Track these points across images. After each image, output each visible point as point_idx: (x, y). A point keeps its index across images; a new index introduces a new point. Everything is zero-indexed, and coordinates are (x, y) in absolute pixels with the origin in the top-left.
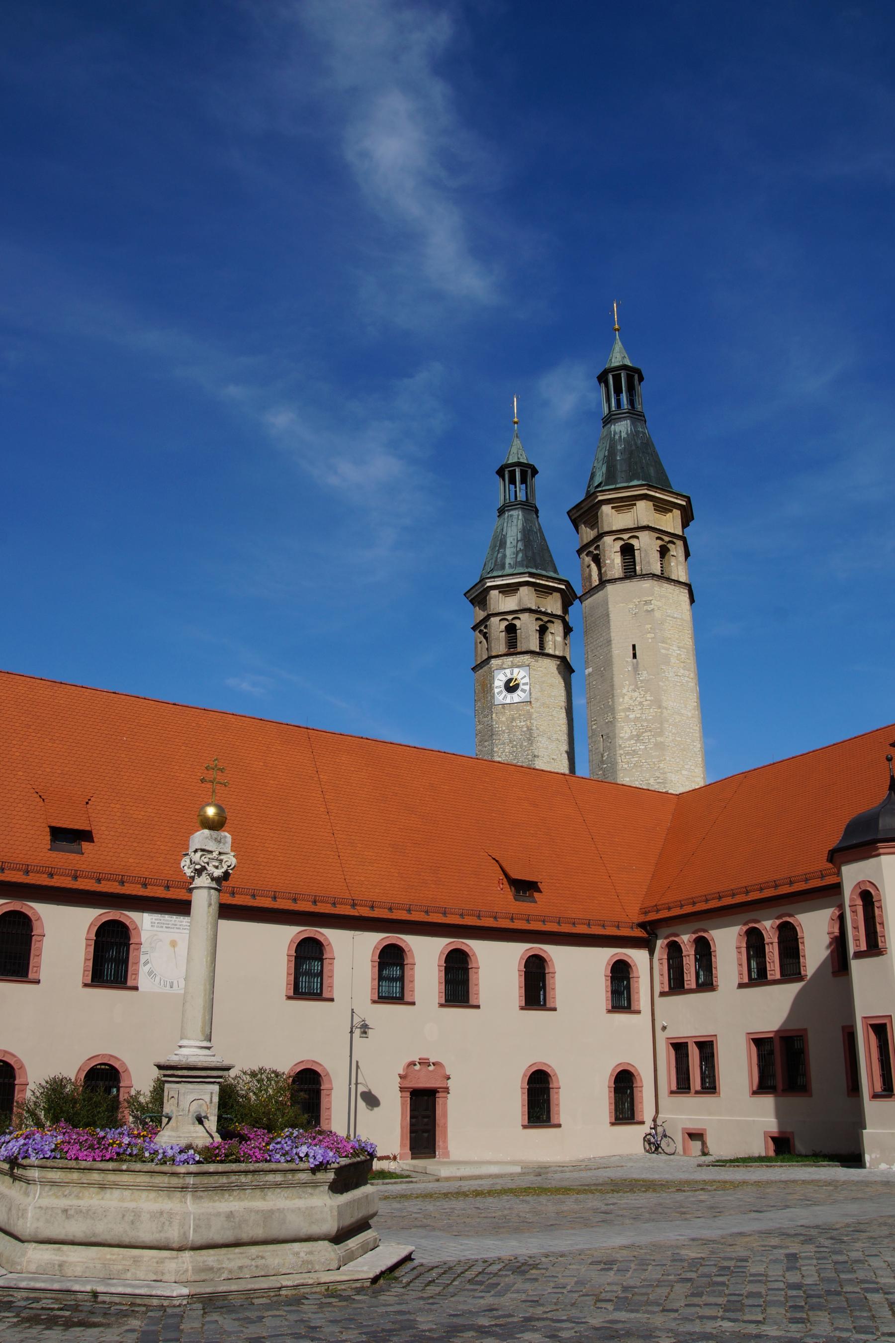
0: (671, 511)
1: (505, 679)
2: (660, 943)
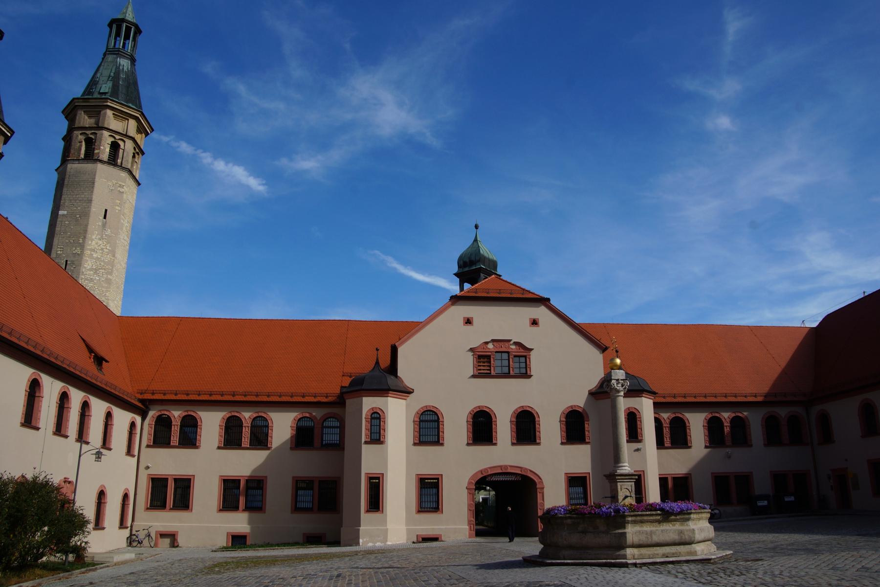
0: (141, 133)
2: (152, 414)
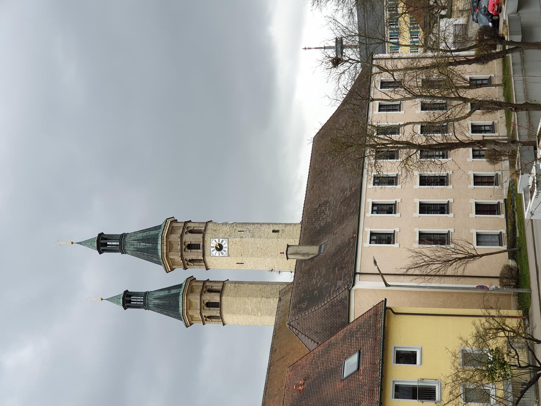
1: (215, 251)
